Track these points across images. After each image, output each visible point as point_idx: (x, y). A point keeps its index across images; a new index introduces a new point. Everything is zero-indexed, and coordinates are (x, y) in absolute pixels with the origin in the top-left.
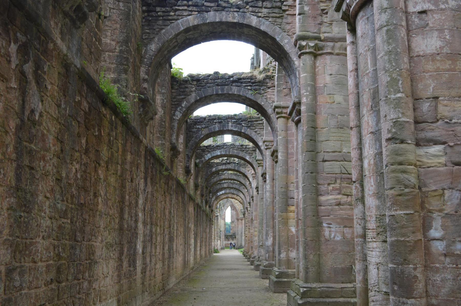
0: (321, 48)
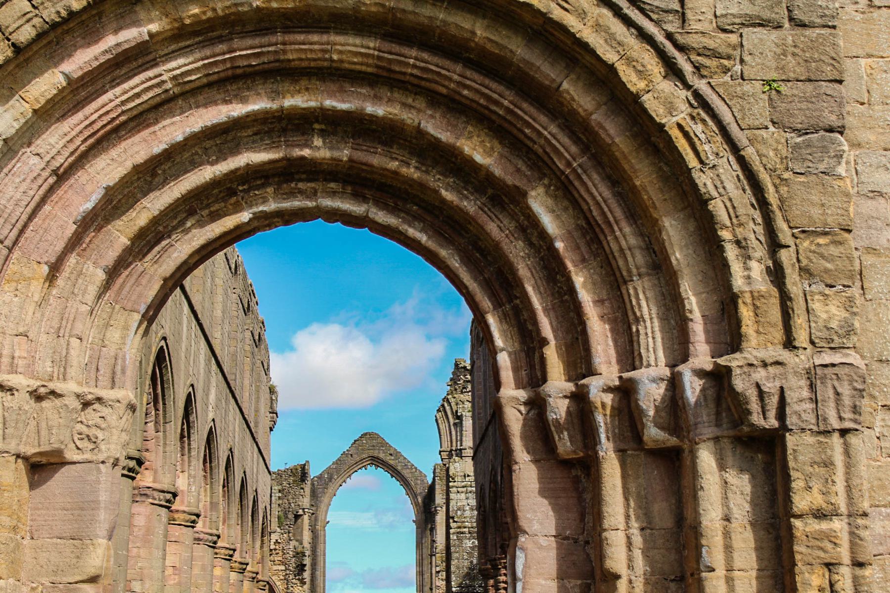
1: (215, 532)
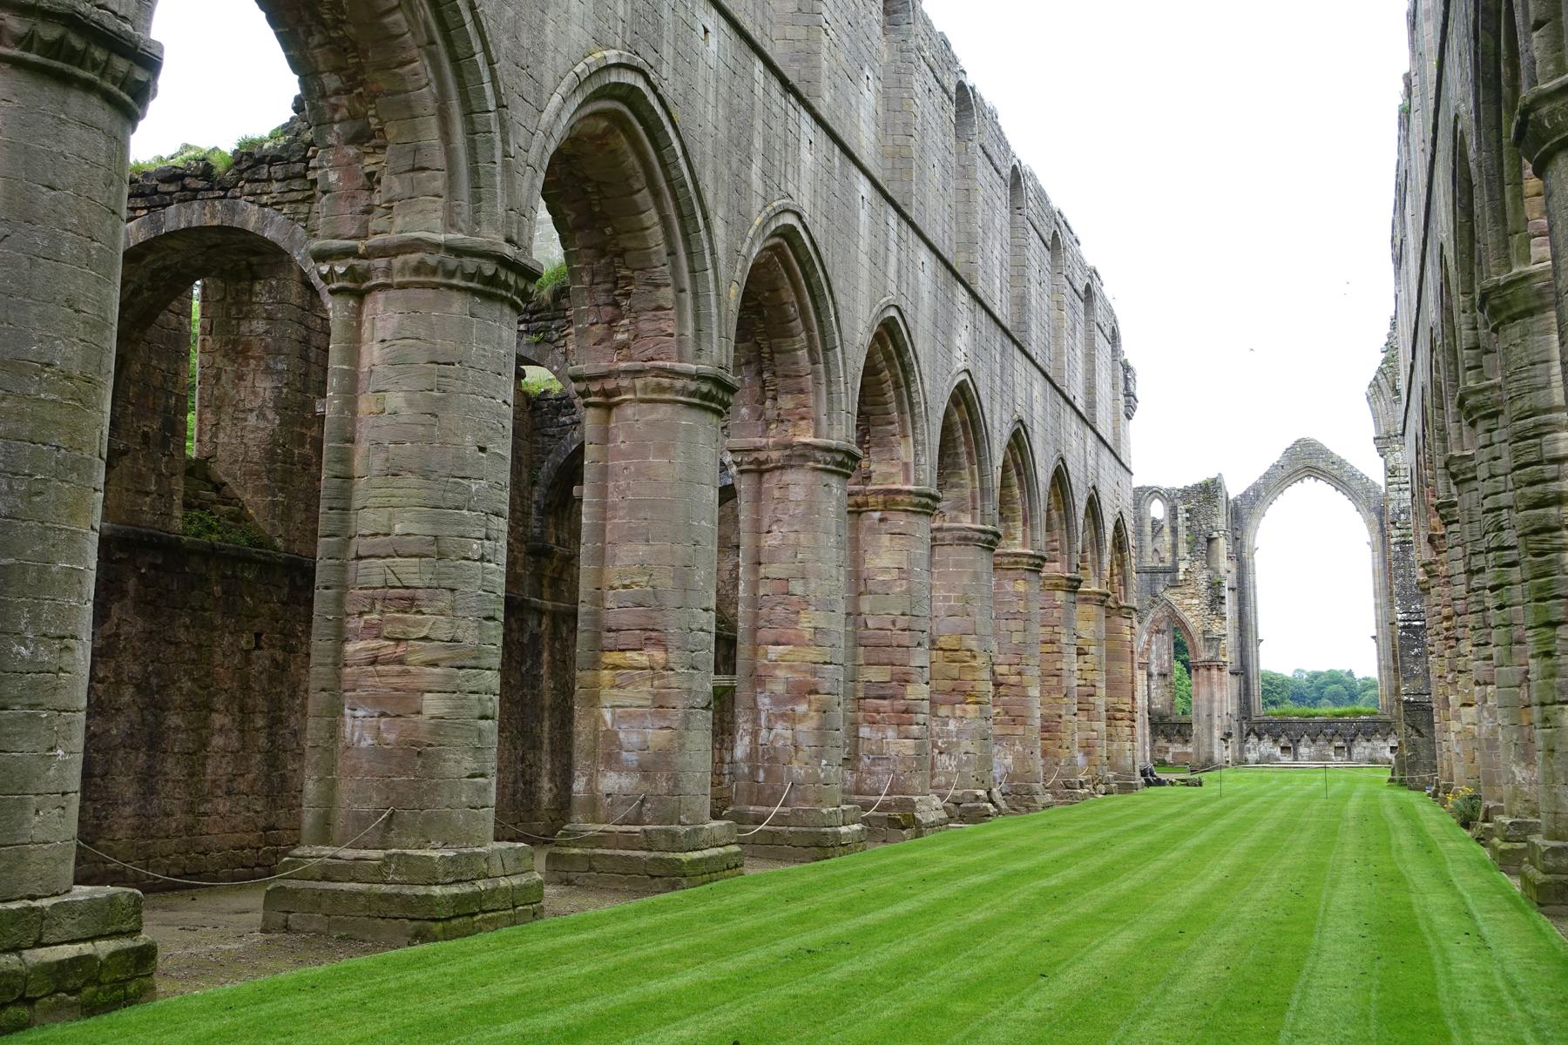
0: (366, 275)
1: (989, 527)
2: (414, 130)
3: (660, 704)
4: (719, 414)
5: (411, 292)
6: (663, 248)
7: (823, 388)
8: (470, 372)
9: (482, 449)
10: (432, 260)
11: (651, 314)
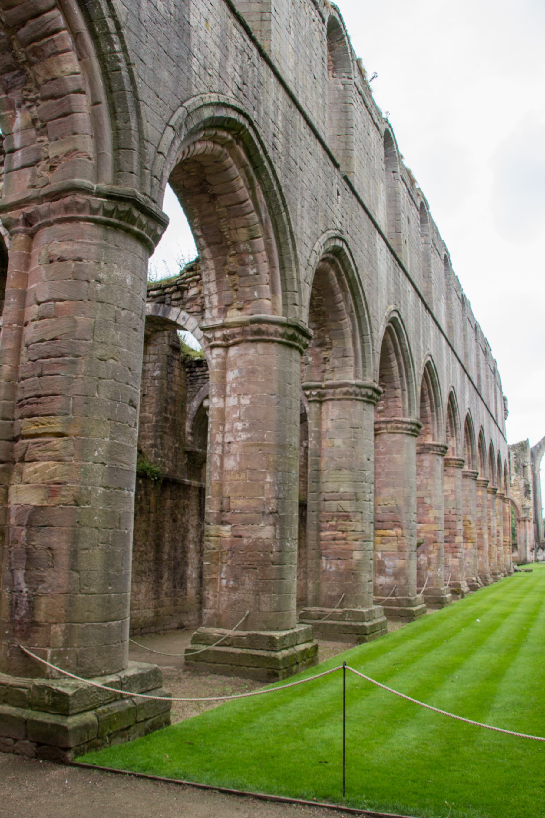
0: (324, 395)
1: (475, 471)
2: (344, 343)
3: (400, 549)
4: (416, 436)
5: (343, 402)
6: (398, 375)
7: (436, 422)
8: (364, 431)
9: (368, 460)
10: (351, 390)
11: (393, 399)
